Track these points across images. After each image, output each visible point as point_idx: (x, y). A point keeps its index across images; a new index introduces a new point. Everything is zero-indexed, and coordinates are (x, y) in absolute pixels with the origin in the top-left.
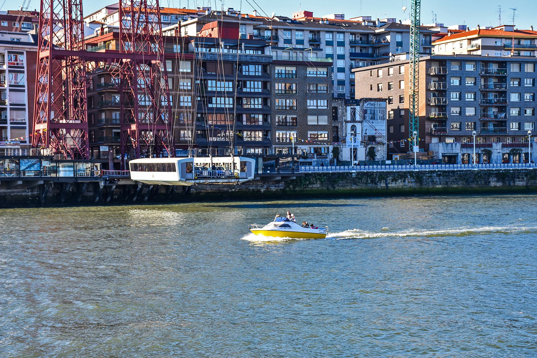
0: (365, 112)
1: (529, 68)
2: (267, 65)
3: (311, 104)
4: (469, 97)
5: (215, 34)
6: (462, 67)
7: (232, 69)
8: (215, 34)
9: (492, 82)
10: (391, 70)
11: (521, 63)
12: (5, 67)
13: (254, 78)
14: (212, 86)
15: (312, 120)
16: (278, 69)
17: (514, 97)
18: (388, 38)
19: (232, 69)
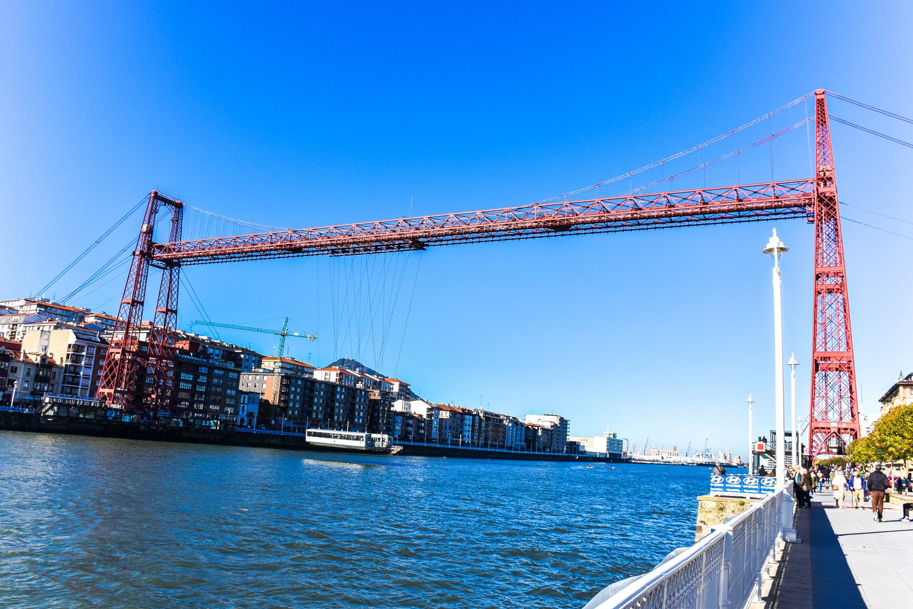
0: (249, 399)
1: (299, 382)
2: (212, 368)
3: (229, 391)
4: (298, 398)
5: (187, 347)
6: (297, 382)
7: (193, 368)
8: (187, 347)
9: (308, 391)
10: (258, 377)
11: (297, 379)
12: (84, 353)
13: (204, 374)
14: (183, 376)
15: (228, 401)
16: (216, 371)
17: (316, 400)
18: (242, 356)
19: (193, 368)
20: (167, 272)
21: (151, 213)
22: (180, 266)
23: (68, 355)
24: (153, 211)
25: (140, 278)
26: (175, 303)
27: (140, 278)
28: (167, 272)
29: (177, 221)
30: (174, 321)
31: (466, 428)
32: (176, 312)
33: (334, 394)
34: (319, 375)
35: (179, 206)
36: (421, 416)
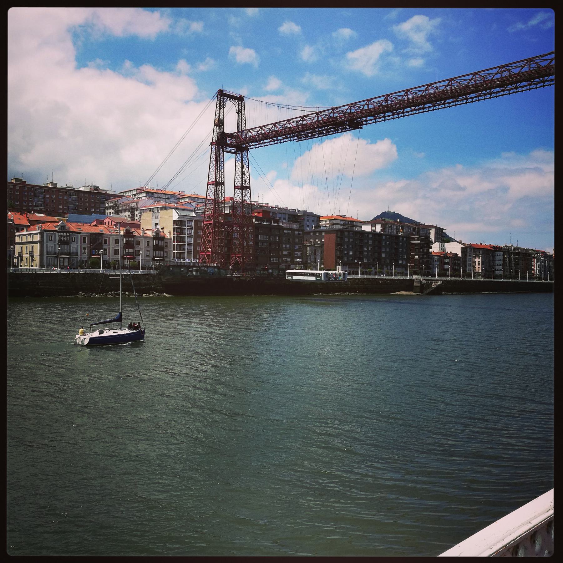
20: (239, 156)
21: (220, 108)
22: (248, 150)
23: (174, 228)
24: (221, 107)
25: (219, 164)
26: (248, 181)
27: (219, 164)
28: (239, 156)
29: (240, 112)
30: (249, 195)
31: (497, 262)
32: (249, 188)
33: (380, 242)
34: (367, 228)
35: (240, 99)
36: (457, 255)
